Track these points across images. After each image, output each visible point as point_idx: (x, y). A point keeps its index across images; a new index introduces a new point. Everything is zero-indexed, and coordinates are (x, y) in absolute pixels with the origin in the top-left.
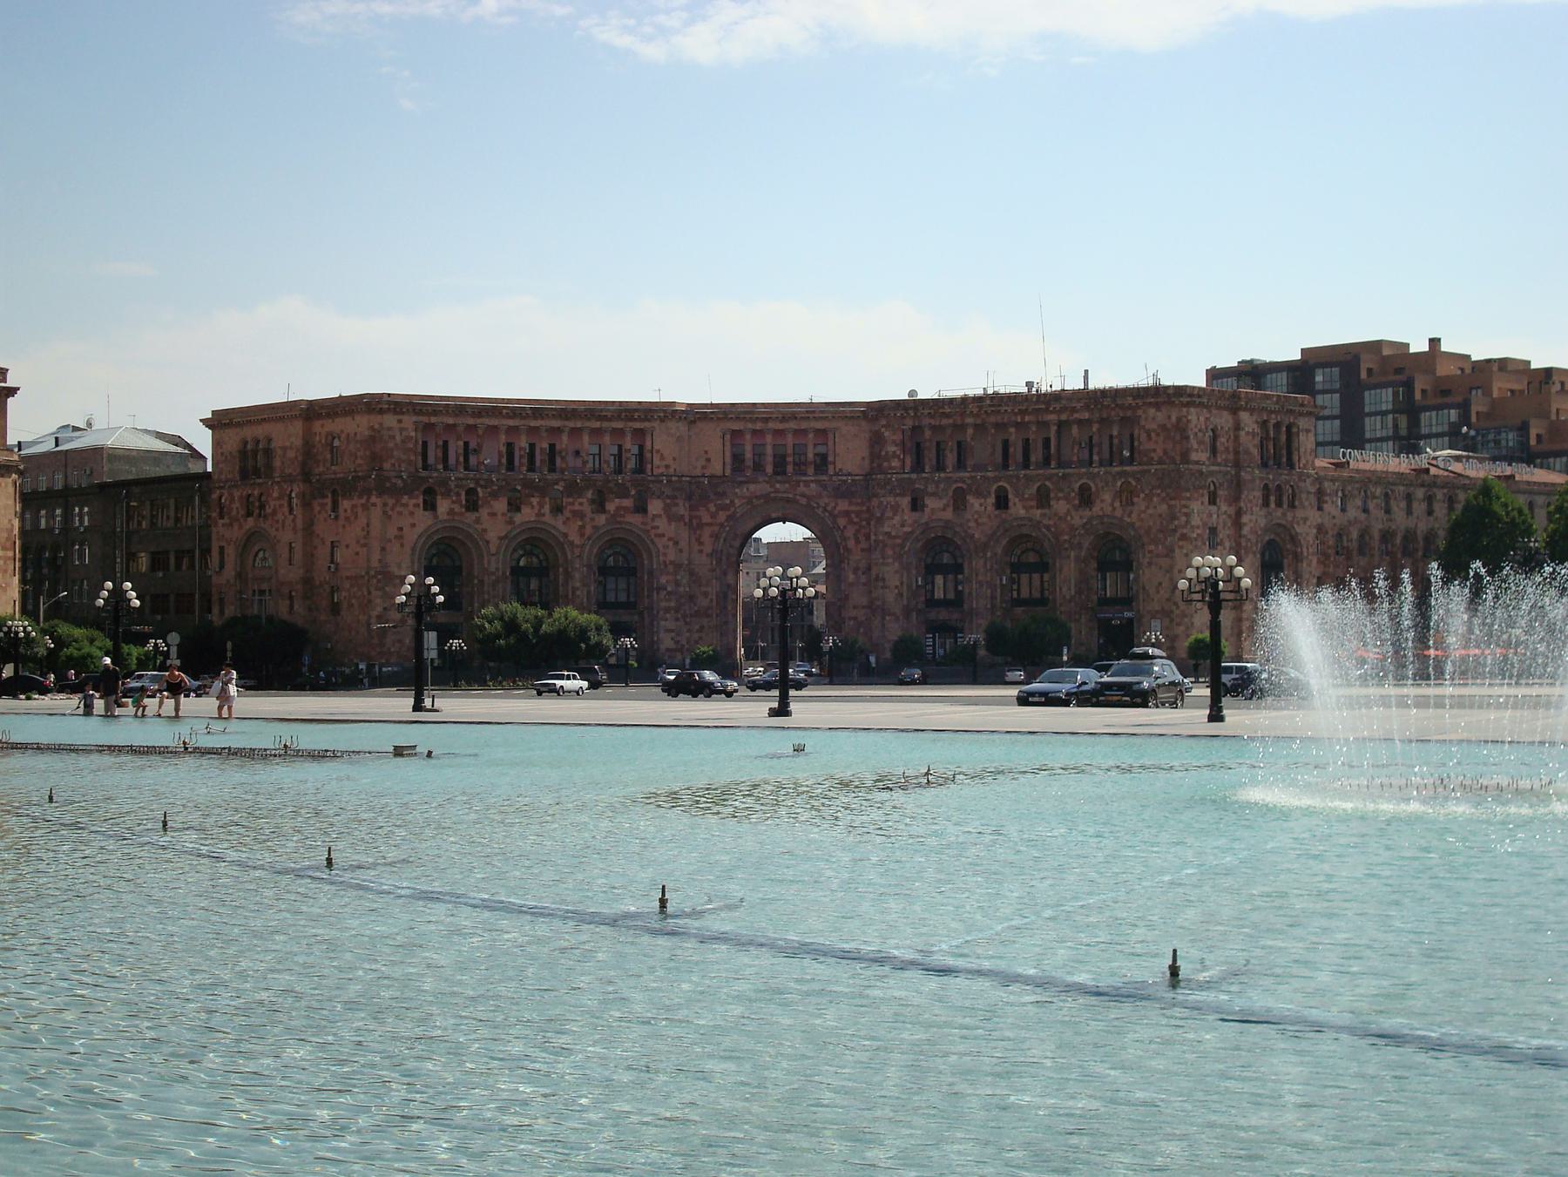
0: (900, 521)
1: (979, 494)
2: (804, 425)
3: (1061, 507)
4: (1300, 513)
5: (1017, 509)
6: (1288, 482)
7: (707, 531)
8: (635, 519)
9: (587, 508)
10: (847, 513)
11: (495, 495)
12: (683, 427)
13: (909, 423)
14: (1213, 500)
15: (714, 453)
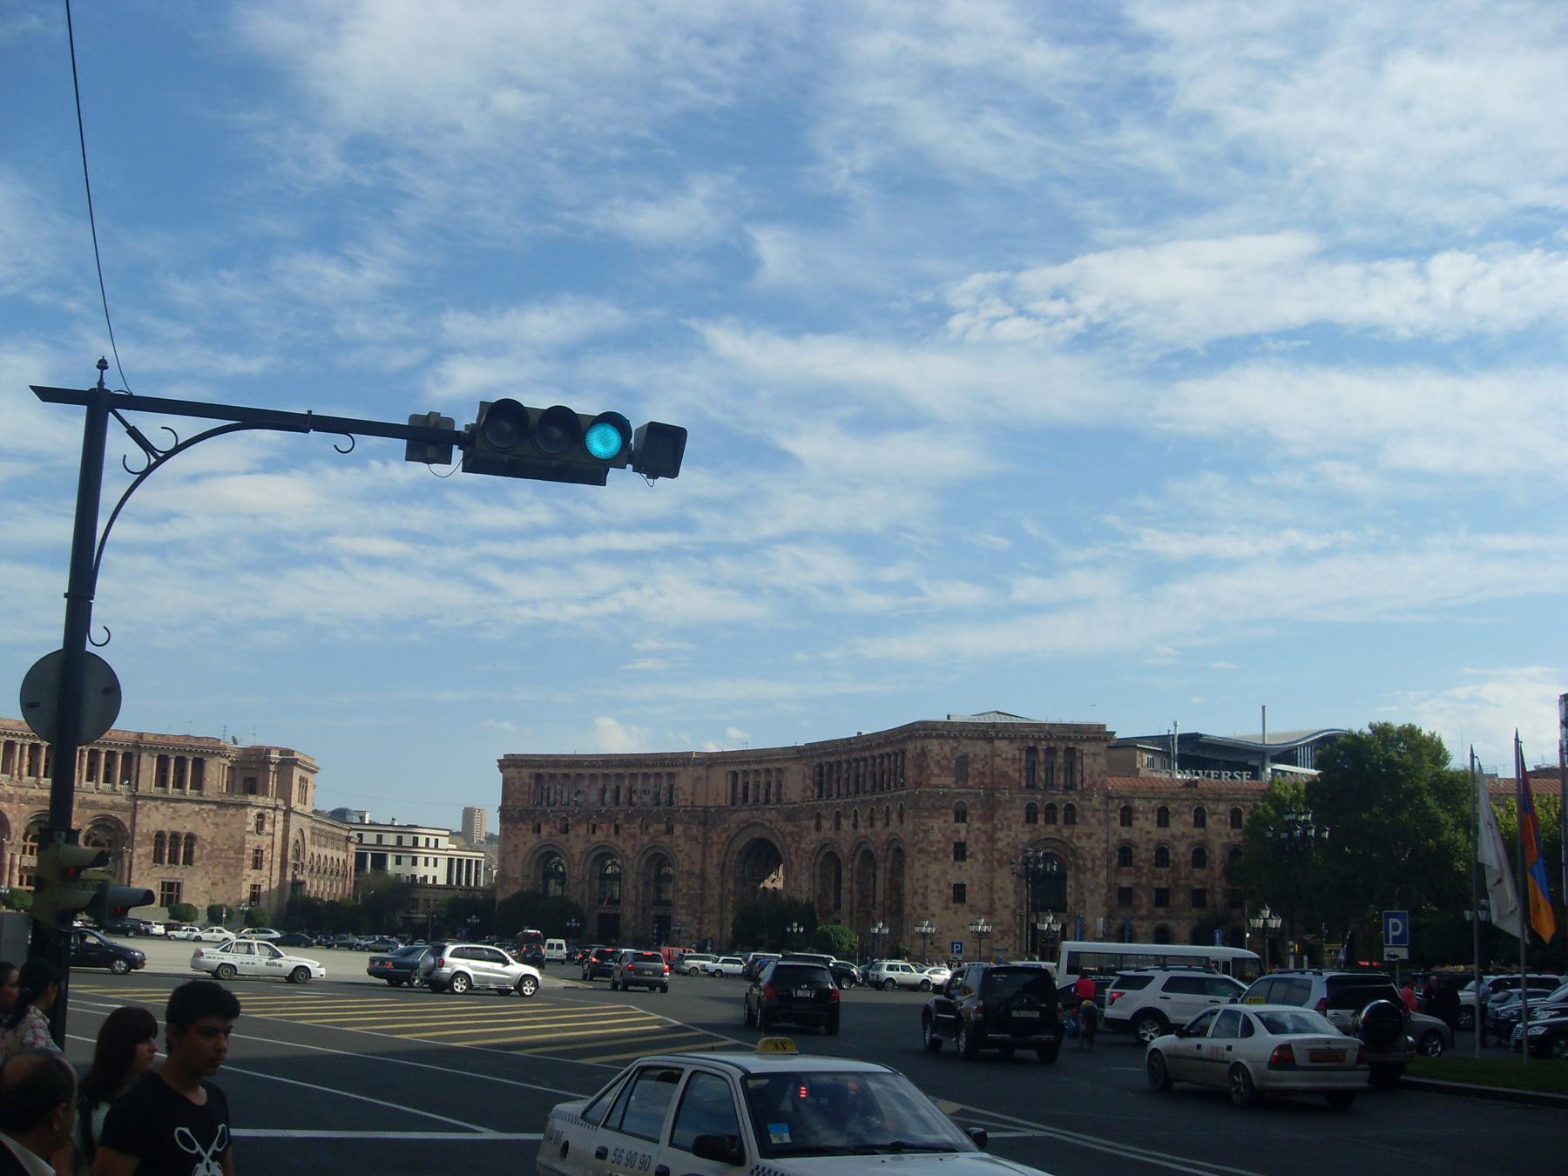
0: (810, 841)
1: (847, 817)
2: (770, 766)
3: (879, 824)
4: (1080, 828)
5: (861, 830)
6: (1062, 801)
7: (715, 848)
8: (665, 839)
9: (638, 831)
10: (791, 834)
11: (579, 822)
12: (701, 771)
13: (817, 761)
14: (961, 816)
15: (719, 787)
